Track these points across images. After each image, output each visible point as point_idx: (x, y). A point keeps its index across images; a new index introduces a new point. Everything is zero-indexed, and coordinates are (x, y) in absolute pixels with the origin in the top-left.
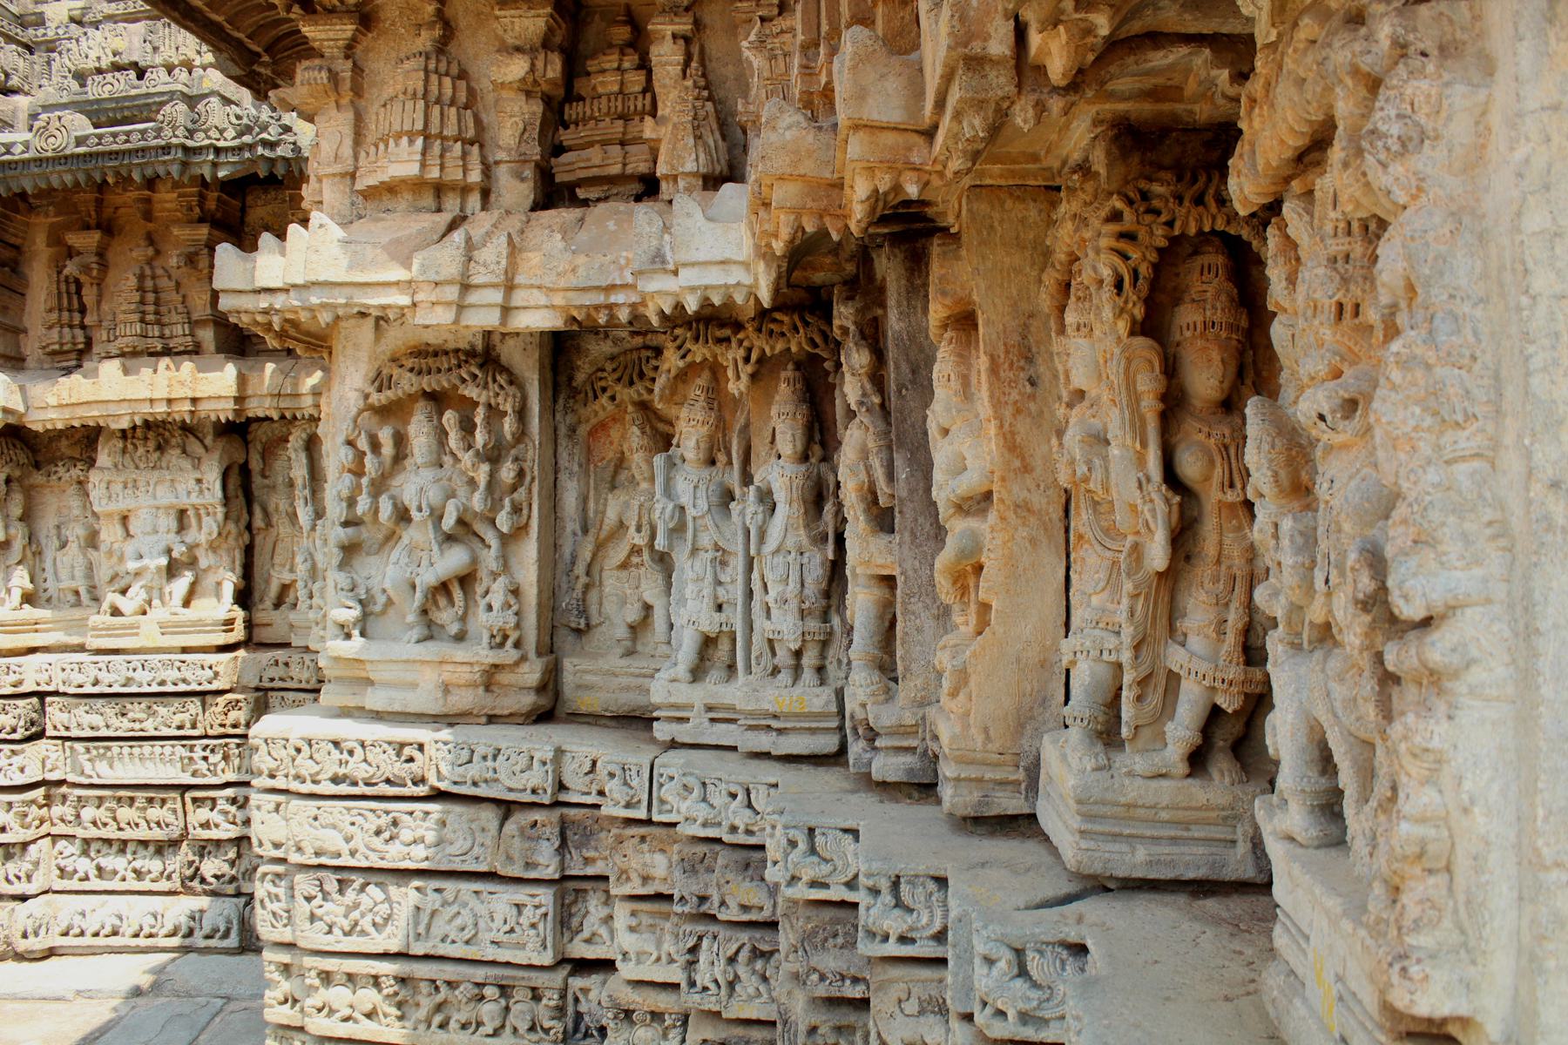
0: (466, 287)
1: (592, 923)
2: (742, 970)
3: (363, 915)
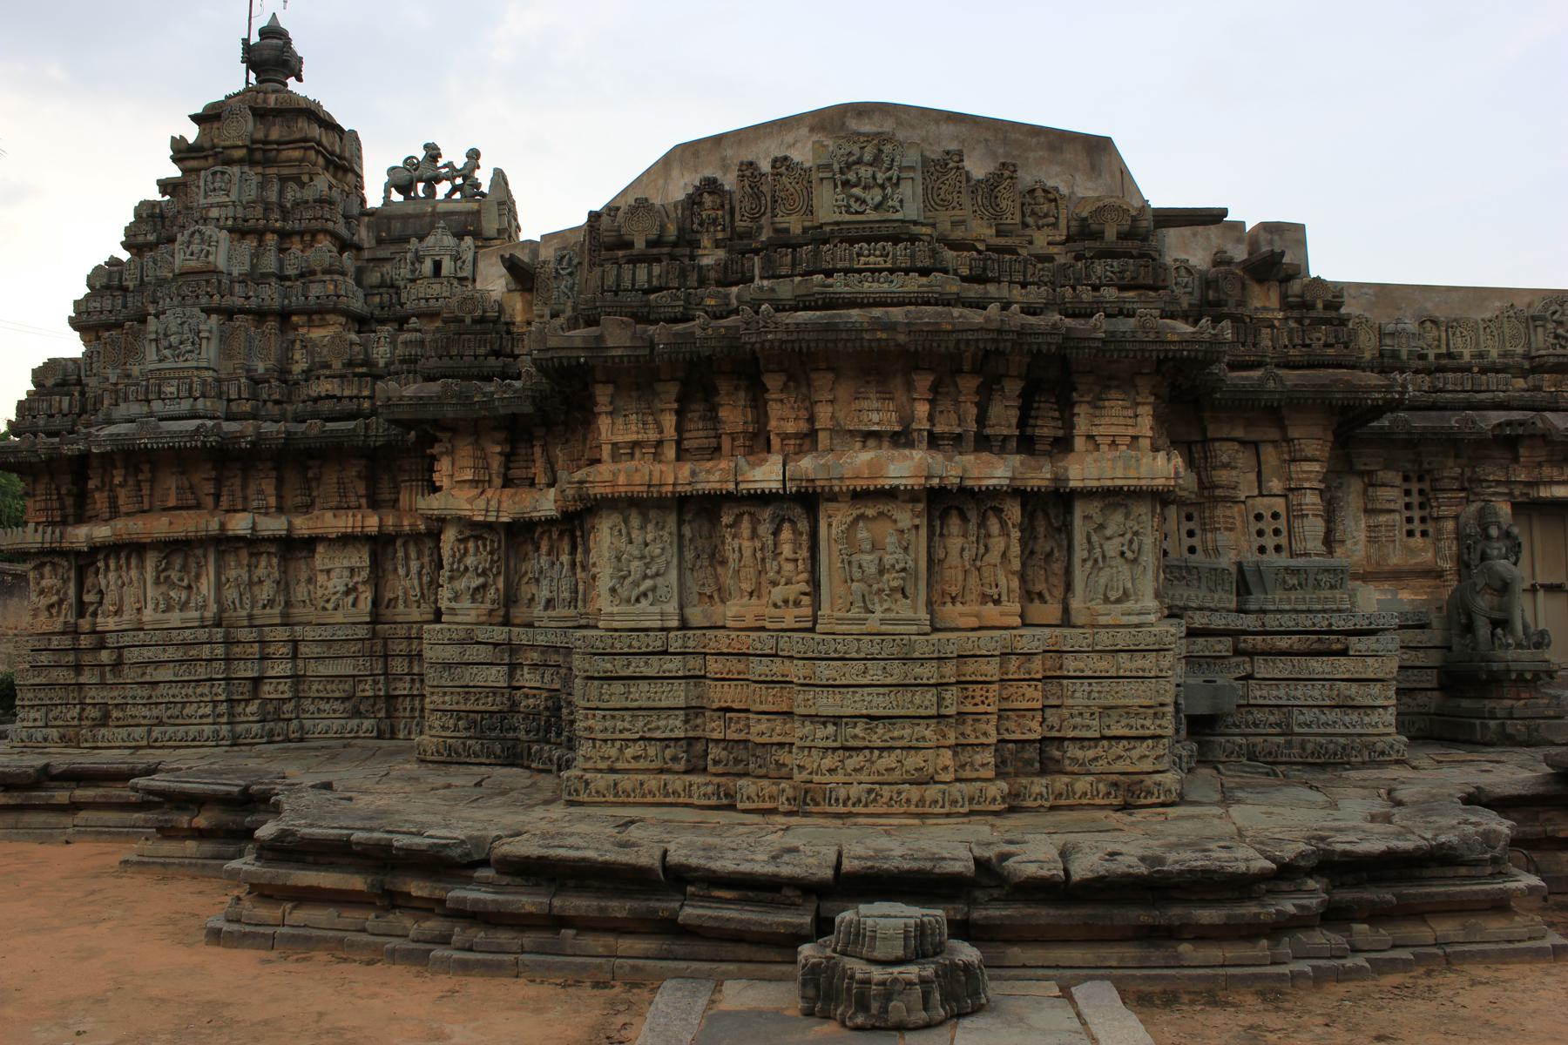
0: (487, 511)
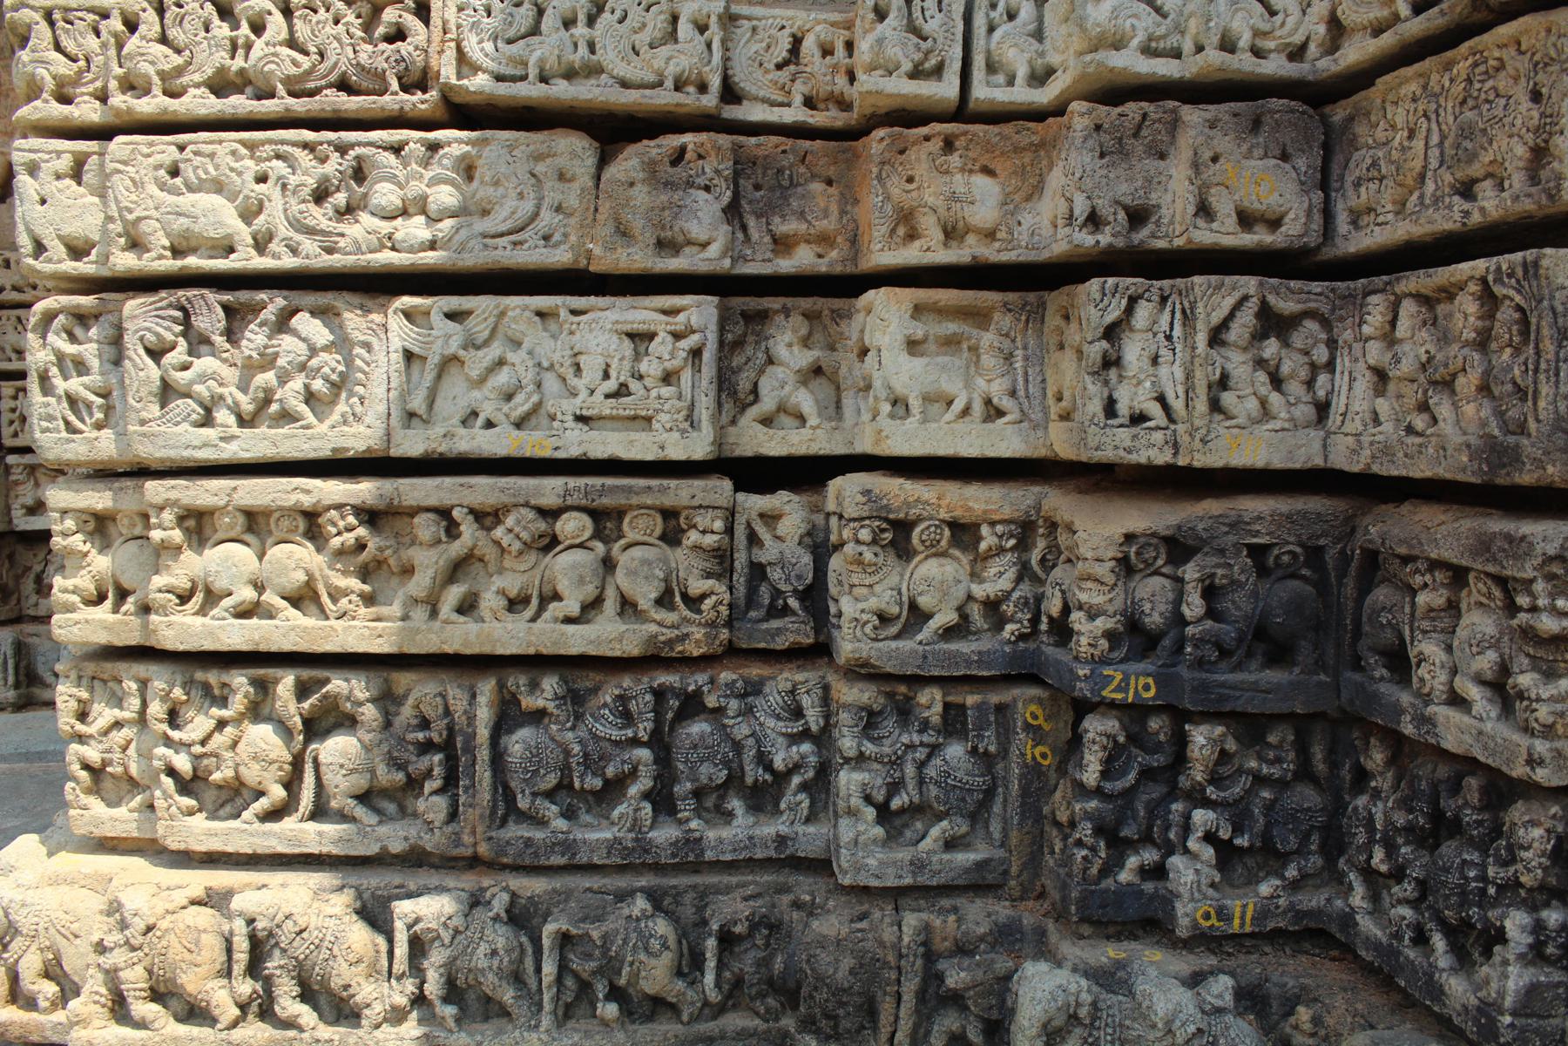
1: (776, 386)
2: (1237, 363)
3: (283, 379)
